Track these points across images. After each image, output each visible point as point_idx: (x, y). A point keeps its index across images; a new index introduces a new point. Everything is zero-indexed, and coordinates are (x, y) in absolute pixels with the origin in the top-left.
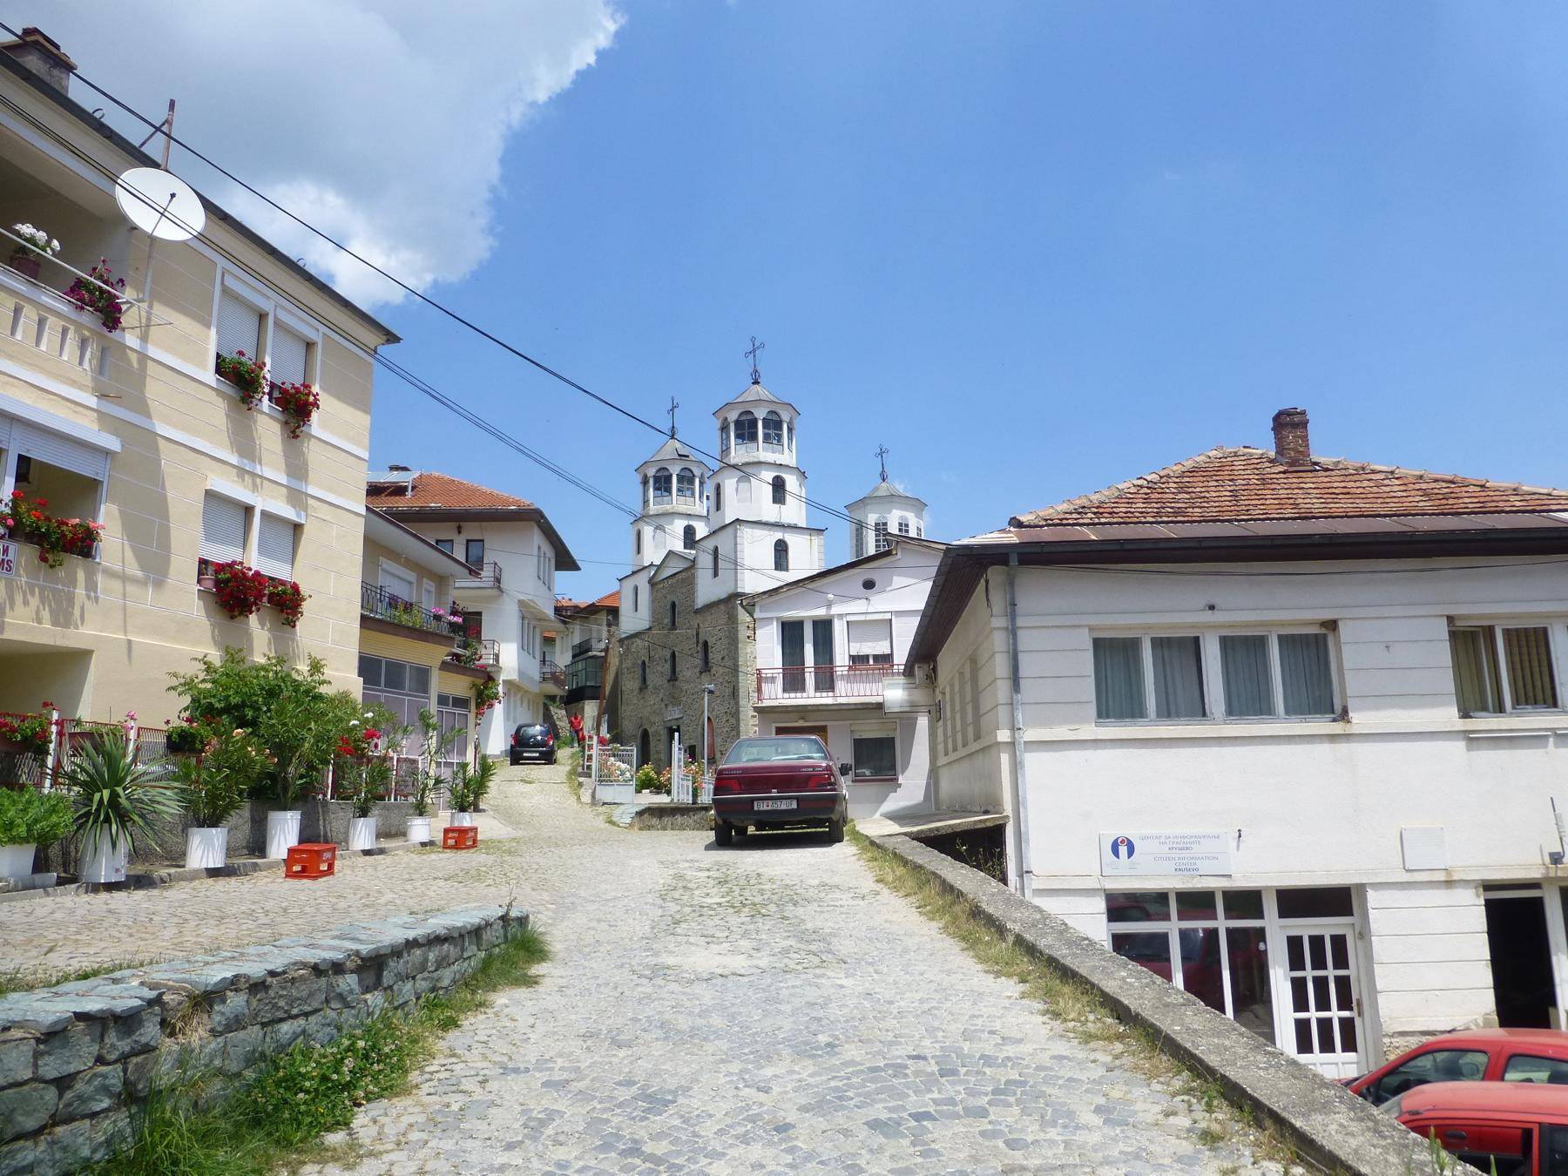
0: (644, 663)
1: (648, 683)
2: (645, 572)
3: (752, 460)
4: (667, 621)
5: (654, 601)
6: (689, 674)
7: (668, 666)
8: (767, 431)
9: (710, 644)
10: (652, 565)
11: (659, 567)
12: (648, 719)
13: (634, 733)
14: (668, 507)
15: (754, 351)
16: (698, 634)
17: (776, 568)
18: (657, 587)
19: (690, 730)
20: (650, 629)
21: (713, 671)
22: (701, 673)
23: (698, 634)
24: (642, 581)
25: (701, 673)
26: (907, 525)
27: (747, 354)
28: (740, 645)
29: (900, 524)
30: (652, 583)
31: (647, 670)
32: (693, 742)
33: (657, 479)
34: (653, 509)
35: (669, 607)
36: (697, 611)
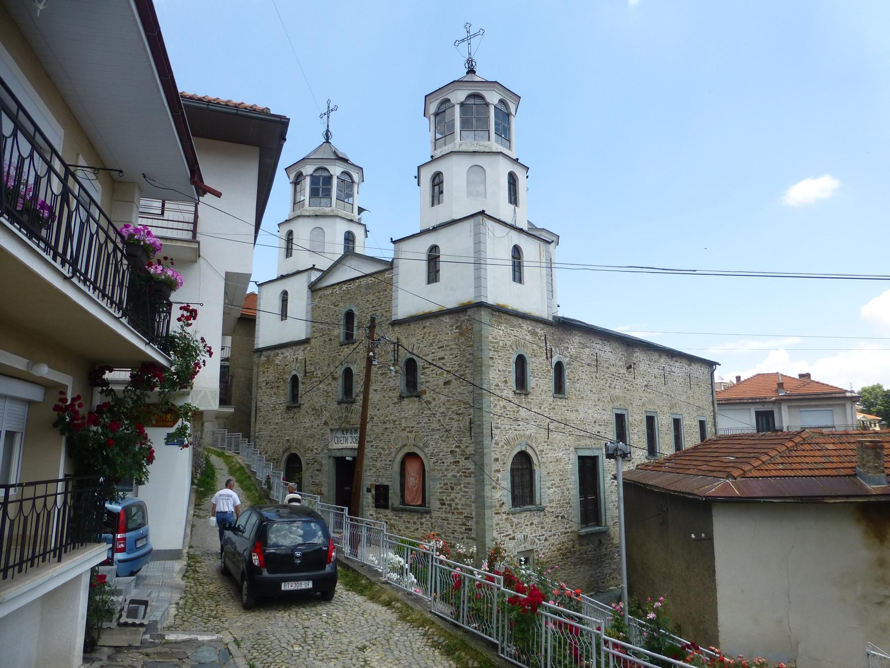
0: (295, 379)
2: (305, 275)
3: (482, 149)
7: (339, 384)
9: (420, 363)
10: (313, 268)
11: (325, 274)
12: (300, 443)
13: (275, 456)
14: (327, 210)
15: (469, 38)
16: (396, 352)
17: (514, 280)
18: (321, 293)
19: (378, 465)
20: (306, 341)
21: (427, 397)
22: (401, 397)
24: (298, 290)
25: (401, 397)
27: (458, 43)
30: (313, 288)
32: (383, 481)
33: (314, 180)
36: (396, 323)
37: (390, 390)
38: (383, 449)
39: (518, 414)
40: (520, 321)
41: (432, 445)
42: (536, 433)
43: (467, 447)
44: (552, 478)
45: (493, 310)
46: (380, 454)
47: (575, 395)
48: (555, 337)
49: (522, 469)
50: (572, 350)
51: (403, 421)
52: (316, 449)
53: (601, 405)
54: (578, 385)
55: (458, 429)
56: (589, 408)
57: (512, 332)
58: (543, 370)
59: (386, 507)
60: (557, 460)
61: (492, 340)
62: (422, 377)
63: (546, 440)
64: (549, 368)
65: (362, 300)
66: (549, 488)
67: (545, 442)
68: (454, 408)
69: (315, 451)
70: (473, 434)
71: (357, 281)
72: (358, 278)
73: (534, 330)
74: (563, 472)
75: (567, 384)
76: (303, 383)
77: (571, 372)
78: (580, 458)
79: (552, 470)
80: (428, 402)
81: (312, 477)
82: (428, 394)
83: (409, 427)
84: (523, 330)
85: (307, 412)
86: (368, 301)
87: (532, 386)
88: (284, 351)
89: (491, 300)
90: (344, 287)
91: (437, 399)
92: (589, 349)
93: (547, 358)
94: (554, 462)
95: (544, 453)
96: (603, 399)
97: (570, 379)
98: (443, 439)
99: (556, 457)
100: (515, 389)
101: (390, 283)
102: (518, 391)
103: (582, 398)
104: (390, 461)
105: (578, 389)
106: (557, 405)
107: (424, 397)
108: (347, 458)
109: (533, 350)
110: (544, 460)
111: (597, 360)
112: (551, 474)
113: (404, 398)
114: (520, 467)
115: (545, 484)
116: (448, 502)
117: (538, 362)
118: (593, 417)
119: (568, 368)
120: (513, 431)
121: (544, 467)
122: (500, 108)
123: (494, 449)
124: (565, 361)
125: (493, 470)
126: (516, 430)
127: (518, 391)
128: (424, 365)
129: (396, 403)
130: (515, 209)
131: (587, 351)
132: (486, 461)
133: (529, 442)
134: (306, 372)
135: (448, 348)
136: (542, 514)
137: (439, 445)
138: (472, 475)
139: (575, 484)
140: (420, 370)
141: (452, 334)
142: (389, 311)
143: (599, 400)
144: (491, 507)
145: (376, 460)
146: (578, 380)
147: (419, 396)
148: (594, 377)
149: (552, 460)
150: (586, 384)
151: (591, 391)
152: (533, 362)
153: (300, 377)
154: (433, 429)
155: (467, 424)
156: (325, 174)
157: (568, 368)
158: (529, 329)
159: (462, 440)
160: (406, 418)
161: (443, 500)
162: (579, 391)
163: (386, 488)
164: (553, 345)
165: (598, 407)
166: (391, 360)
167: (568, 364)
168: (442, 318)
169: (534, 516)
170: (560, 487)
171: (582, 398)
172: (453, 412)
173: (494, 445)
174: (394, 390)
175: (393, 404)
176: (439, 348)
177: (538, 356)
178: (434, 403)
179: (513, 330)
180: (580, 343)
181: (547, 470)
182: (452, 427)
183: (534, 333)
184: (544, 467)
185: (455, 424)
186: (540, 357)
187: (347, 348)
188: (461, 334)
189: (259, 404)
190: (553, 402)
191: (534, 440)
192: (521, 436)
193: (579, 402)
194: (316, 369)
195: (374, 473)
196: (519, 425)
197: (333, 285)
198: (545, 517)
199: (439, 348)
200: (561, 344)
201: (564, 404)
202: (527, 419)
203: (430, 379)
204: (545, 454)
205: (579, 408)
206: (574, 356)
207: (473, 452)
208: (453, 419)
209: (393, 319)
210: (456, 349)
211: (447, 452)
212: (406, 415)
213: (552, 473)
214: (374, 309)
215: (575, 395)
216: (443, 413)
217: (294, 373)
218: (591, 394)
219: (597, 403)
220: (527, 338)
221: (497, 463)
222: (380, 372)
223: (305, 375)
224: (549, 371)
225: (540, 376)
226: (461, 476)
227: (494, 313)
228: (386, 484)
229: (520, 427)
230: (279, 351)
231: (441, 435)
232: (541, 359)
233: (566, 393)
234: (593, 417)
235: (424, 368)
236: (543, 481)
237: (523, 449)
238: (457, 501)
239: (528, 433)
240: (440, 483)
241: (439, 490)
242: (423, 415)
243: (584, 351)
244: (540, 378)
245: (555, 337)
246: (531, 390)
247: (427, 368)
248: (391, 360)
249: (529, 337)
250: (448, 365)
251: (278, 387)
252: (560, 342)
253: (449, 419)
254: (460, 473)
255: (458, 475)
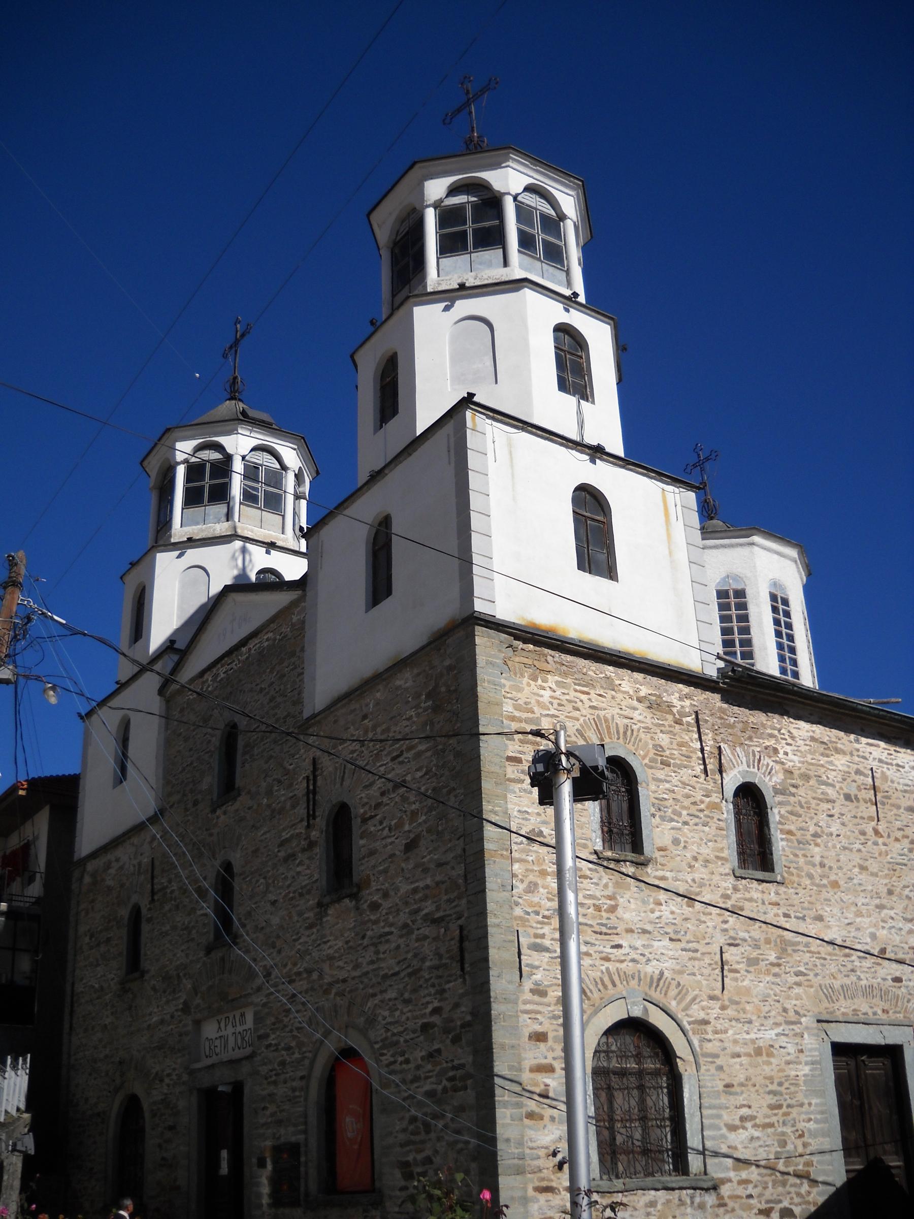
0: (136, 915)
1: (145, 964)
4: (209, 781)
5: (169, 739)
6: (275, 920)
8: (523, 227)
16: (312, 793)
17: (581, 567)
21: (371, 895)
22: (322, 907)
23: (312, 793)
25: (322, 907)
26: (785, 602)
28: (487, 785)
29: (774, 597)
31: (145, 928)
32: (289, 1135)
34: (179, 530)
35: (216, 741)
37: (301, 895)
38: (288, 1048)
39: (612, 916)
40: (610, 670)
41: (385, 1019)
42: (681, 972)
43: (457, 1005)
44: (741, 1100)
45: (517, 638)
46: (283, 1063)
47: (810, 876)
48: (732, 720)
49: (640, 1073)
50: (791, 756)
51: (326, 967)
52: (169, 1075)
53: (899, 907)
54: (817, 849)
55: (436, 962)
56: (859, 914)
57: (584, 697)
58: (694, 803)
59: (295, 1204)
60: (758, 1052)
61: (517, 714)
62: (362, 842)
63: (718, 992)
64: (715, 798)
65: (251, 690)
66: (732, 1128)
67: (712, 998)
68: (429, 907)
69: (167, 1081)
70: (467, 967)
71: (244, 649)
72: (244, 642)
73: (660, 696)
74: (780, 1084)
75: (780, 845)
76: (149, 920)
77: (791, 813)
78: (840, 1050)
79: (741, 1078)
80: (375, 906)
81: (160, 1146)
82: (374, 886)
83: (337, 982)
84: (620, 696)
85: (154, 989)
86: (261, 690)
87: (659, 843)
88: (119, 852)
89: (504, 611)
90: (221, 671)
91: (392, 893)
92: (848, 758)
93: (705, 771)
94: (749, 1055)
95: (709, 1028)
96: (907, 892)
97: (790, 832)
98: (406, 996)
99: (753, 1041)
100: (599, 846)
101: (300, 629)
102: (609, 854)
103: (835, 885)
104: (302, 1078)
105: (817, 859)
106: (750, 900)
107: (365, 892)
108: (220, 1089)
109: (659, 748)
110: (709, 1047)
111: (874, 788)
112: (737, 1089)
113: (327, 906)
114: (632, 1065)
115: (719, 1117)
116: (419, 1169)
117: (675, 781)
118: (873, 936)
119: (780, 803)
120: (598, 962)
121: (712, 1068)
122: (533, 205)
123: (529, 1007)
124: (768, 783)
125: (527, 1064)
126: (607, 959)
127: (609, 854)
128: (365, 813)
129: (310, 927)
130: (579, 412)
131: (840, 762)
132: (499, 1036)
133: (656, 996)
134: (153, 893)
135: (410, 755)
136: (710, 1199)
137: (397, 1013)
138: (469, 1082)
139: (825, 1121)
140: (356, 823)
141: (418, 715)
142: (298, 702)
143: (890, 893)
144: (520, 1171)
145: (275, 1083)
146: (816, 835)
147: (354, 896)
148: (870, 831)
149: (738, 1049)
150: (845, 848)
151: (863, 868)
152: (660, 781)
153: (144, 904)
154: (385, 977)
155: (455, 944)
156: (215, 456)
157: (780, 803)
158: (642, 694)
159: (444, 991)
160: (331, 958)
161: (406, 1164)
162: (822, 865)
163: (294, 1149)
164: (723, 740)
165: (892, 913)
166: (302, 820)
167: (777, 792)
168: (398, 683)
169: (682, 1203)
170: (771, 1125)
171: (835, 885)
172: (426, 918)
173: (528, 996)
174: (309, 892)
175: (308, 928)
176: (393, 759)
177: (675, 765)
178: (386, 904)
179: (588, 693)
180: (813, 739)
181: (723, 1076)
182: (423, 960)
183: (655, 705)
184: (712, 1068)
185: (427, 949)
186: (680, 767)
187: (225, 813)
188: (436, 709)
189: (79, 988)
190: (736, 889)
191: (673, 992)
192: (626, 977)
193: (824, 895)
194: (170, 881)
195: (272, 1115)
196: (619, 946)
197: (202, 673)
198: (722, 1210)
199: (393, 759)
200: (750, 738)
201: (773, 897)
202: (645, 932)
203: (378, 845)
204: (716, 1032)
205: (826, 911)
206: (796, 772)
207: (468, 1018)
208: (426, 937)
209: (305, 718)
210: (427, 750)
211: (414, 1032)
212: (331, 951)
213: (742, 1085)
214: (272, 704)
215: (810, 876)
216: (406, 926)
217: (135, 898)
218: (864, 877)
219: (884, 901)
220: (636, 715)
221: (542, 1045)
222: (282, 854)
223: (153, 900)
224: (714, 807)
225: (687, 818)
226: (445, 1090)
227: (519, 644)
228: (293, 1139)
229: (621, 951)
230: (110, 856)
231: (401, 986)
232: (685, 774)
233: (777, 868)
234: (873, 936)
235: (365, 820)
236: (710, 1107)
237: (637, 1012)
238: (437, 1160)
239: (651, 969)
240: (402, 1119)
241: (402, 1137)
242: (366, 942)
243: (831, 763)
244: (686, 823)
245: (732, 720)
246: (657, 854)
247: (372, 817)
248: (302, 820)
249: (641, 714)
250: (412, 799)
251: (108, 940)
252: (749, 733)
253: (417, 940)
254: (445, 1082)
255: (440, 1087)
